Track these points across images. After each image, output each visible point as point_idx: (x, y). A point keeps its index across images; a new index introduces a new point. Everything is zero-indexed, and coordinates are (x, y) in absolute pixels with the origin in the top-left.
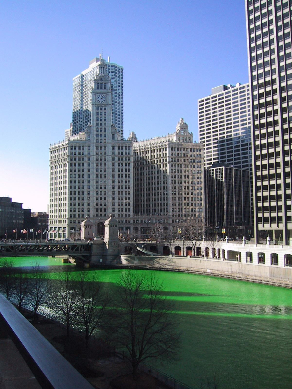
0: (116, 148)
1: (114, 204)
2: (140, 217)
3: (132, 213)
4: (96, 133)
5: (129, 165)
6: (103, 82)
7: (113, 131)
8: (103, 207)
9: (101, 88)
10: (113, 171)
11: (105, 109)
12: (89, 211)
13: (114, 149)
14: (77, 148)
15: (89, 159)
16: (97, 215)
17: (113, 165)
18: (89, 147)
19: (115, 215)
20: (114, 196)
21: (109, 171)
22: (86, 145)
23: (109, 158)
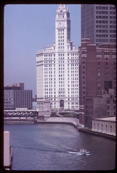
7: (68, 44)
8: (63, 91)
13: (68, 55)
14: (48, 56)
16: (60, 96)
18: (54, 55)
23: (66, 61)
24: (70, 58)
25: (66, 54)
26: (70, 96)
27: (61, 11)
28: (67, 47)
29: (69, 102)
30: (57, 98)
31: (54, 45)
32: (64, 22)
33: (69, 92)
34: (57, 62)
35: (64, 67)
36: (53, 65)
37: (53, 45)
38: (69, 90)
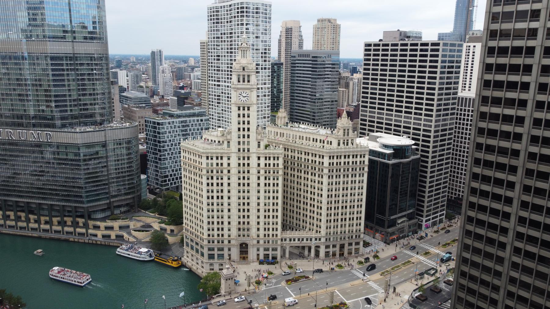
0: (262, 159)
1: (258, 223)
2: (289, 234)
3: (279, 232)
4: (237, 140)
5: (278, 179)
6: (246, 74)
7: (259, 137)
9: (244, 81)
11: (248, 109)
12: (229, 230)
14: (215, 158)
15: (229, 171)
16: (239, 236)
17: (259, 178)
20: (258, 214)
21: (253, 185)
22: (225, 155)
23: (253, 171)
24: (262, 165)
27: (244, 69)
29: (258, 247)
32: (252, 91)
33: (258, 229)
34: (234, 171)
36: (225, 178)
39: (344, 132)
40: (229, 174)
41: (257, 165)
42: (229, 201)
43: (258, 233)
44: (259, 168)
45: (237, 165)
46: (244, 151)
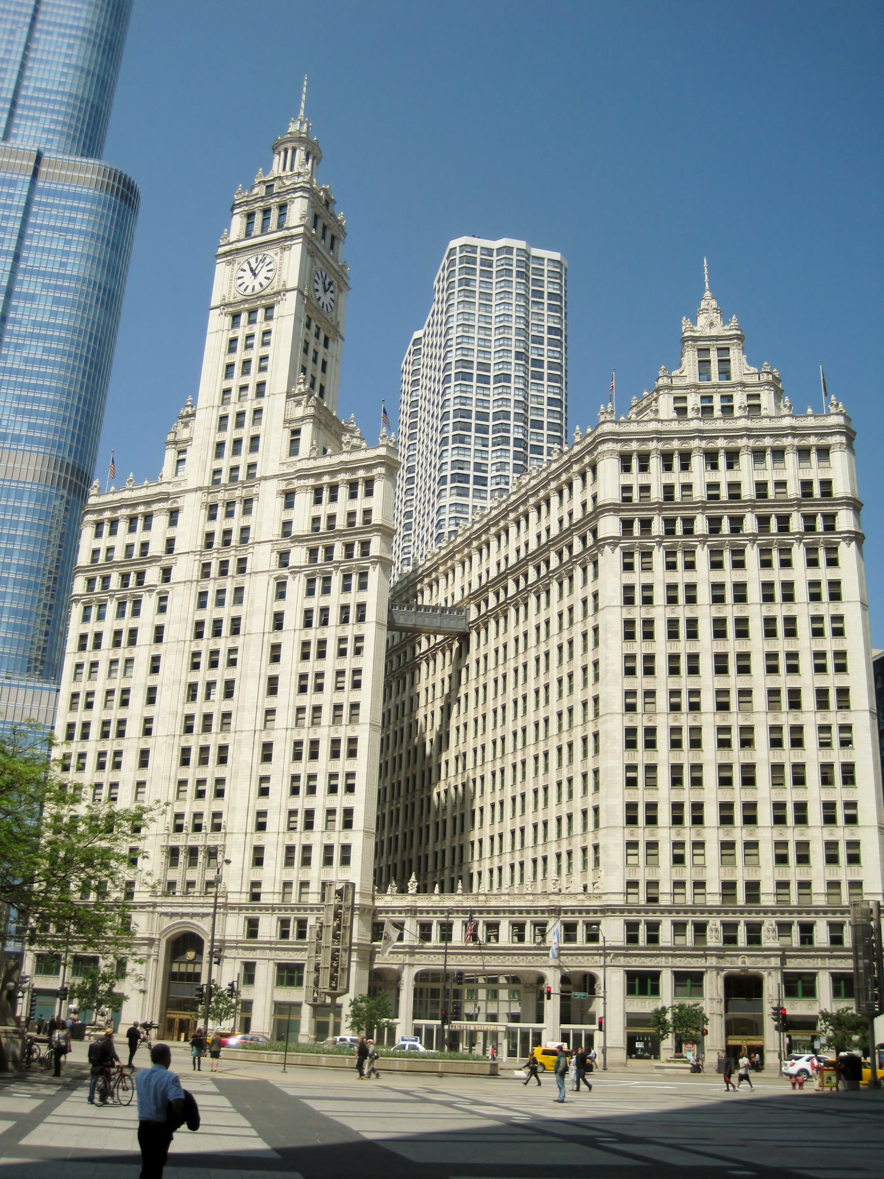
0: (304, 500)
3: (358, 872)
7: (299, 412)
10: (278, 622)
13: (289, 505)
15: (166, 573)
18: (174, 515)
19: (264, 888)
23: (262, 558)
24: (302, 526)
25: (268, 498)
26: (270, 895)
28: (287, 434)
29: (249, 956)
30: (143, 906)
31: (184, 434)
34: (185, 568)
35: (235, 611)
36: (149, 603)
37: (170, 437)
38: (261, 827)
39: (704, 364)
40: (166, 587)
41: (278, 529)
42: (150, 711)
43: (256, 874)
44: (286, 544)
45: (200, 541)
46: (233, 479)
